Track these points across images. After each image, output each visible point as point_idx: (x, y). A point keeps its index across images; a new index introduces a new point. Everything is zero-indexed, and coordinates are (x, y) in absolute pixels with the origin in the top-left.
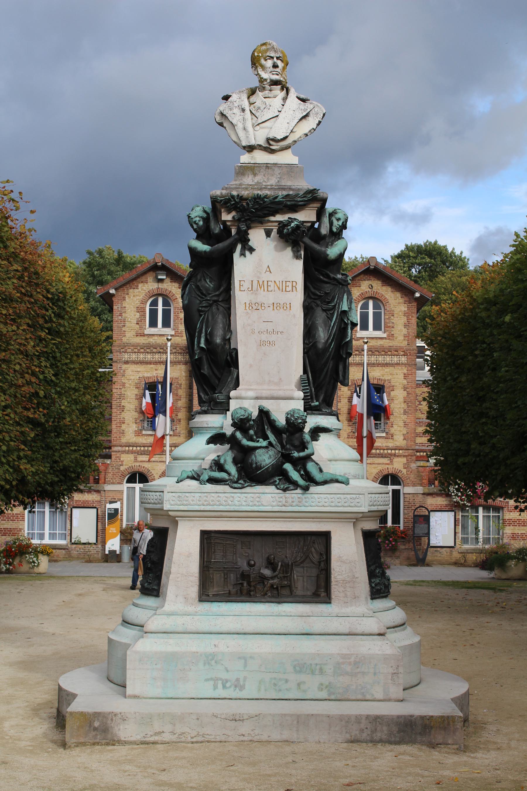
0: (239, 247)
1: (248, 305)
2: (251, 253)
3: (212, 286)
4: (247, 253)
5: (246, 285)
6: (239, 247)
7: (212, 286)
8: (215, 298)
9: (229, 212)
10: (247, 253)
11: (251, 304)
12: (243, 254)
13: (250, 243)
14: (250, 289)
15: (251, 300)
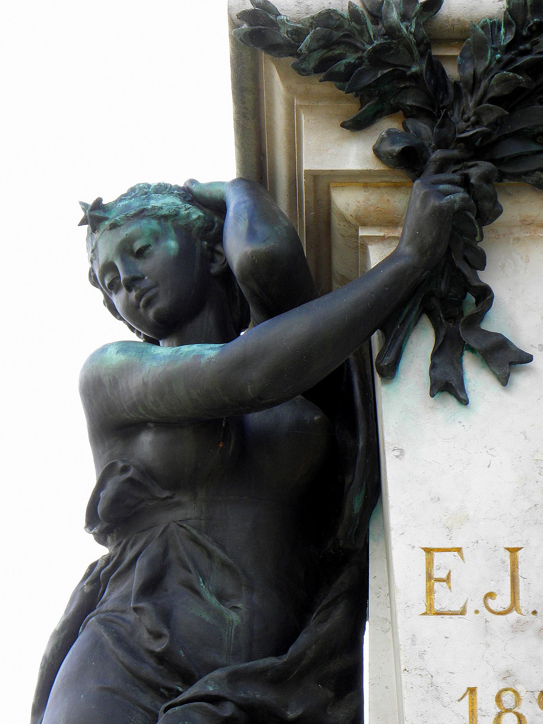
0: (422, 345)
1: (487, 705)
2: (504, 381)
3: (234, 617)
4: (477, 377)
5: (475, 576)
6: (422, 345)
7: (234, 617)
8: (256, 694)
9: (356, 125)
10: (477, 377)
11: (508, 699)
12: (447, 385)
13: (494, 323)
14: (503, 601)
15: (508, 675)
